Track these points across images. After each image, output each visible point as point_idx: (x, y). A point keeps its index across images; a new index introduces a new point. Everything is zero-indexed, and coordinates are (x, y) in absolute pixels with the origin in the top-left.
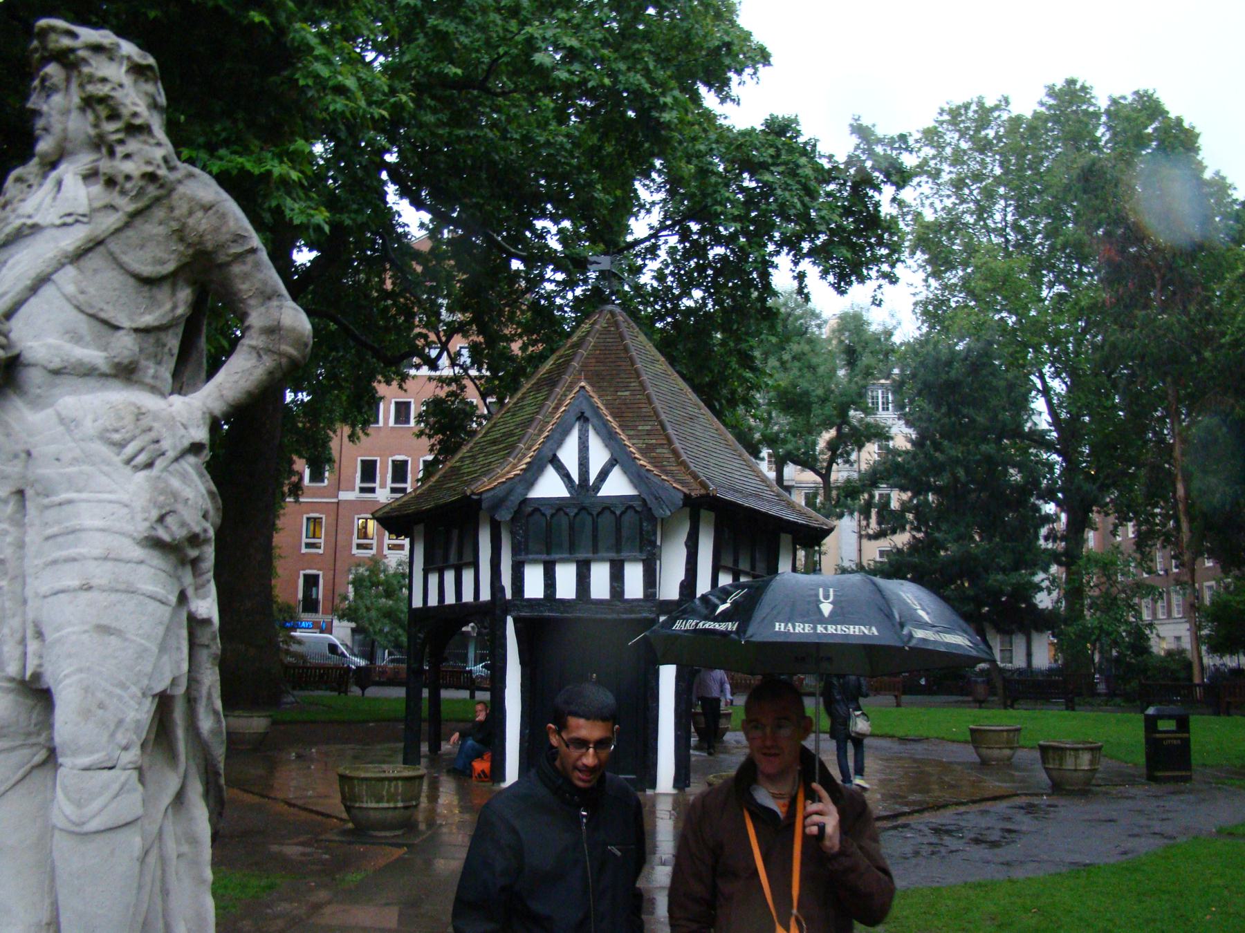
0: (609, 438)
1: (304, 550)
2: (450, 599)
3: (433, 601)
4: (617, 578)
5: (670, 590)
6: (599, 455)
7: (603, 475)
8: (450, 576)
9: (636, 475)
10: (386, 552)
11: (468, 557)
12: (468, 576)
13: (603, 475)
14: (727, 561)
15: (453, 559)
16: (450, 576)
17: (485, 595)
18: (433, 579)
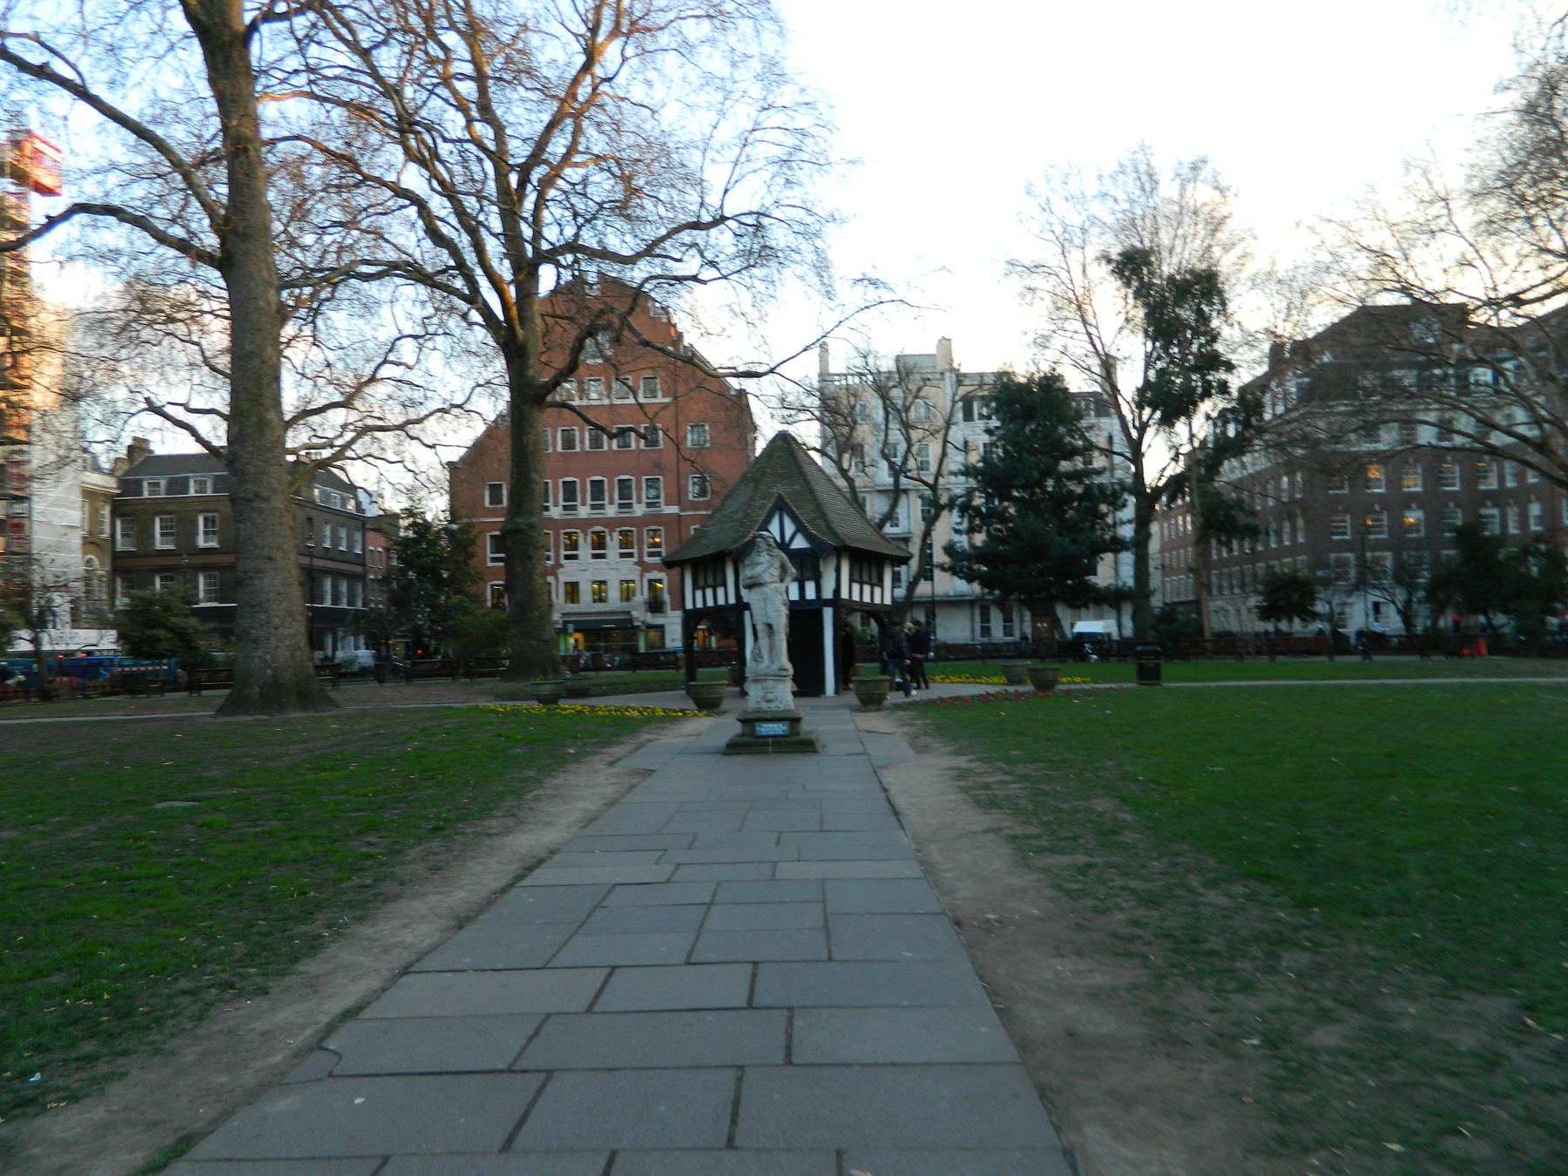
0: (795, 519)
1: (490, 564)
2: (710, 603)
3: (699, 605)
4: (802, 590)
5: (828, 594)
6: (790, 528)
7: (792, 539)
8: (709, 592)
9: (809, 537)
10: (563, 561)
11: (719, 580)
12: (720, 591)
13: (792, 539)
14: (856, 577)
15: (710, 581)
16: (709, 592)
17: (732, 600)
18: (699, 594)
